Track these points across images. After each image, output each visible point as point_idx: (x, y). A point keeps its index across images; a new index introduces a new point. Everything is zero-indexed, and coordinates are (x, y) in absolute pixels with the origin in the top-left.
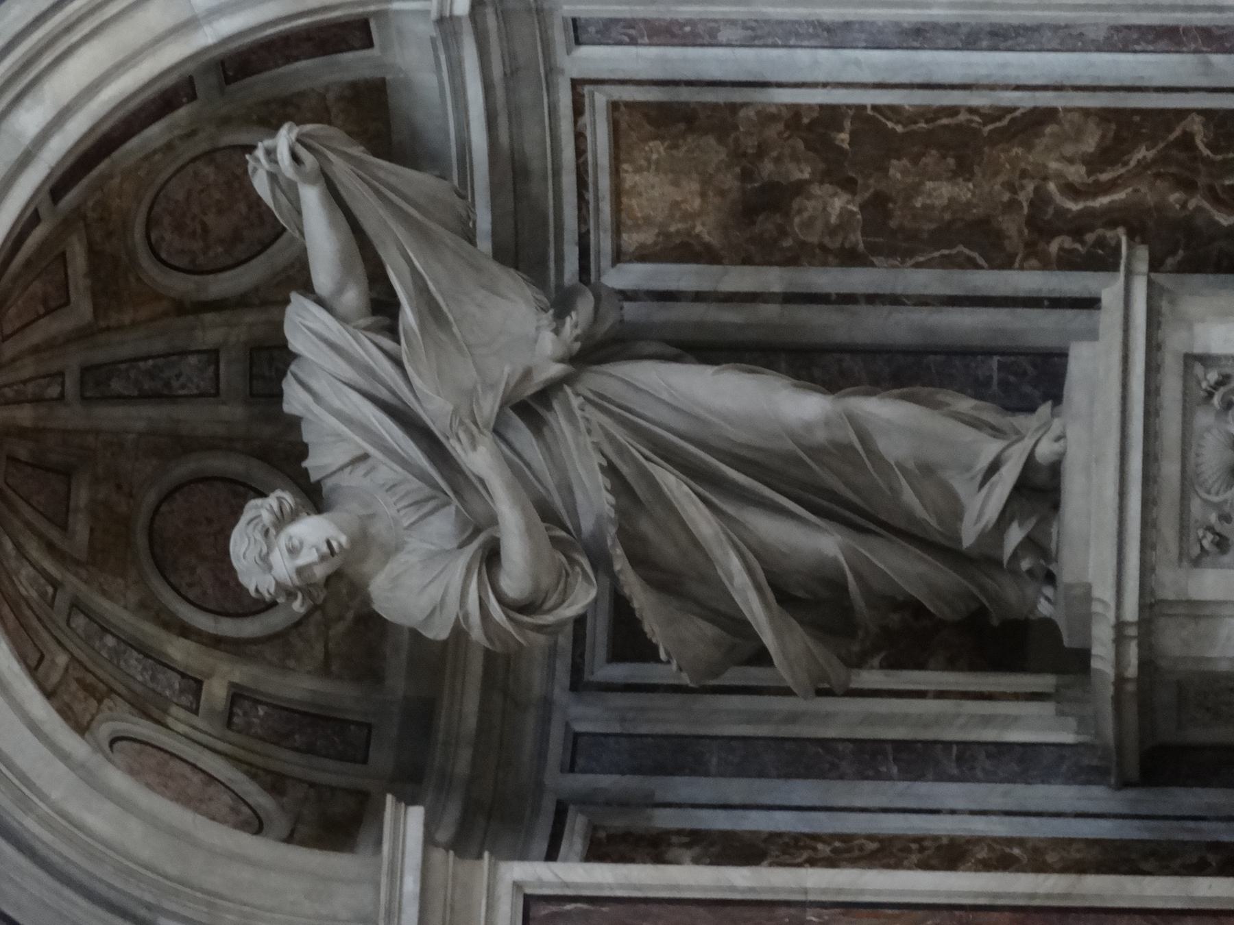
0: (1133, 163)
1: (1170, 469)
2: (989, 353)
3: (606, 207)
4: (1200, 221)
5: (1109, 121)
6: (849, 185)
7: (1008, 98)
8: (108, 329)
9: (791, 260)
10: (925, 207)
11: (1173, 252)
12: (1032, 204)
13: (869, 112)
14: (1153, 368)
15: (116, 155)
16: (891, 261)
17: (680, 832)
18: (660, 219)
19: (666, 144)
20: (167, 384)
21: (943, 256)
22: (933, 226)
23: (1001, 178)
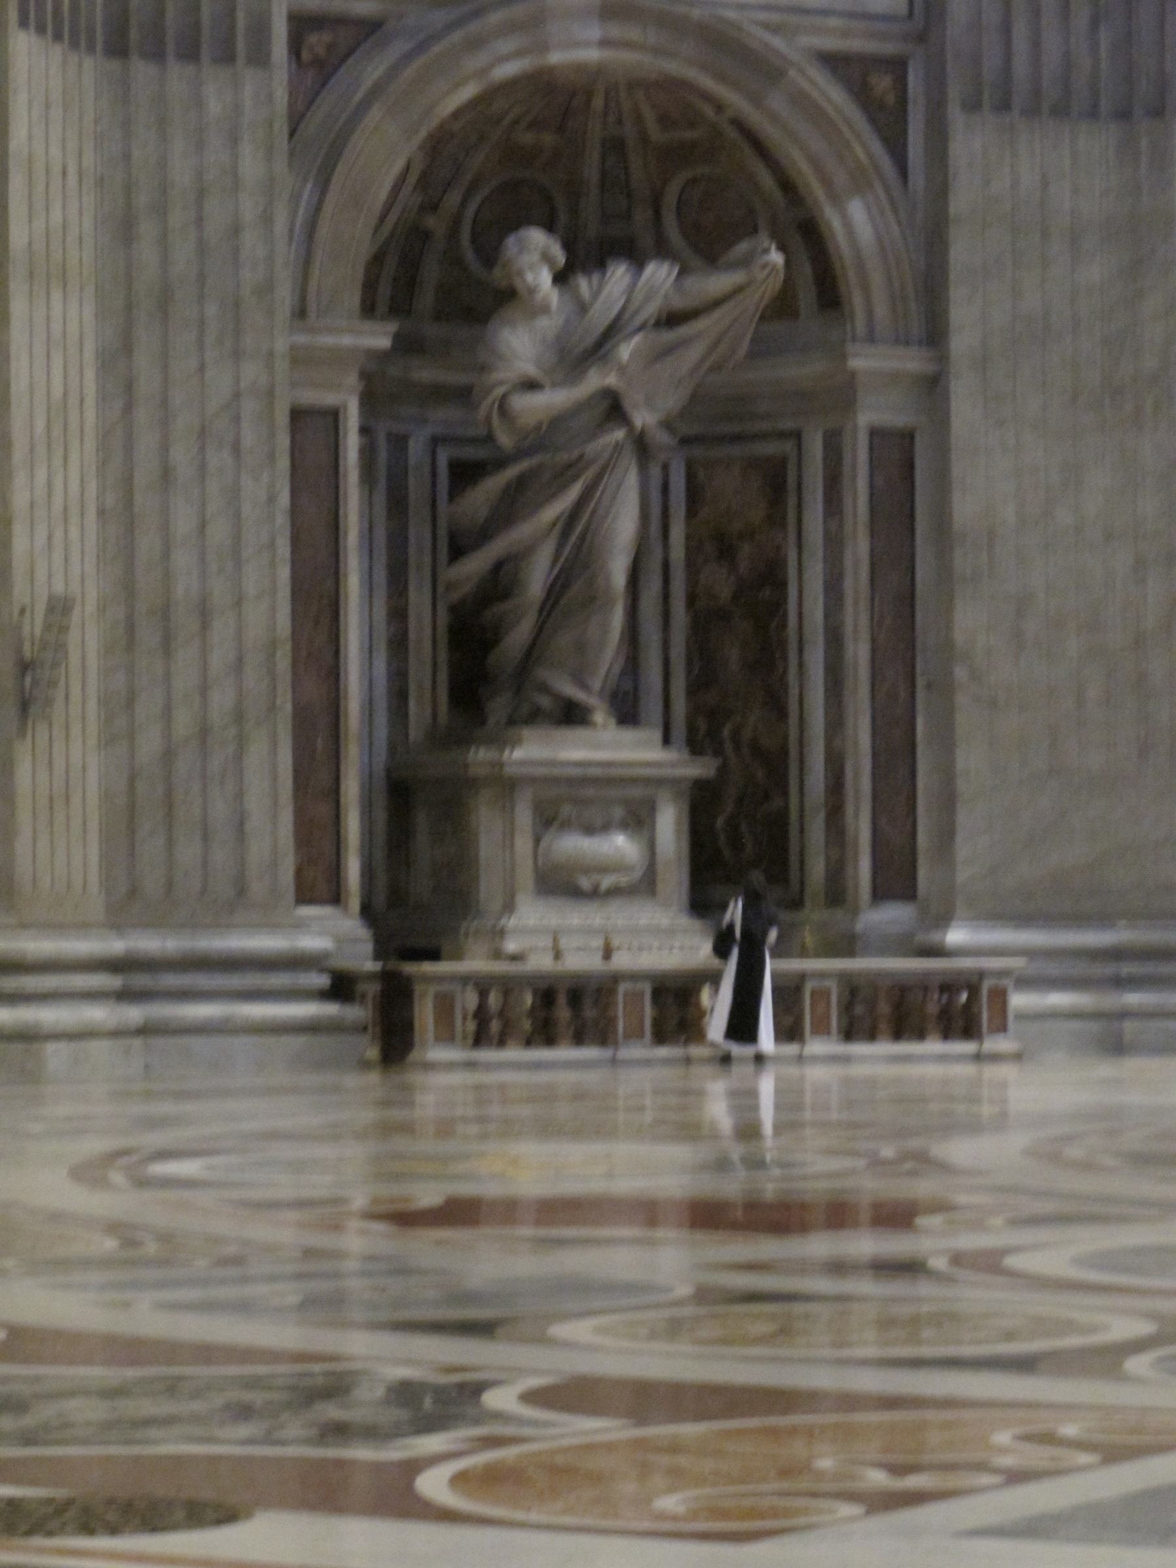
6: (735, 597)
7: (794, 692)
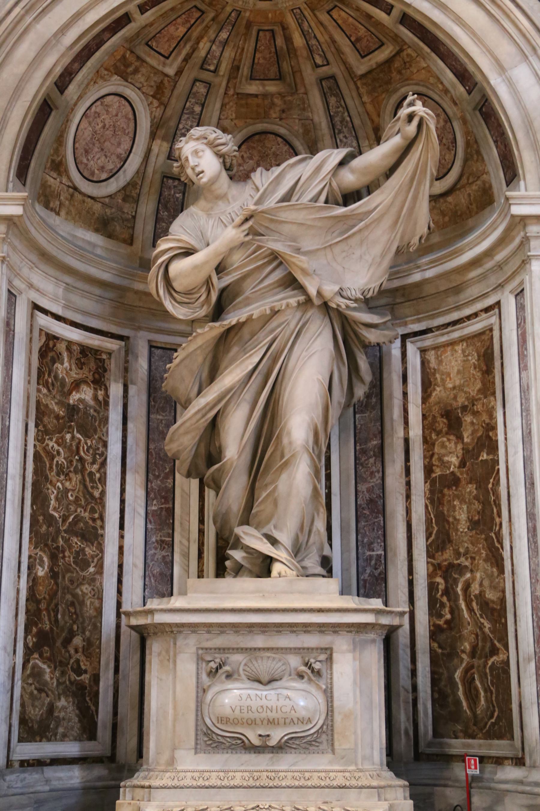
0: (482, 620)
1: (259, 641)
2: (385, 550)
3: (444, 339)
5: (501, 605)
6: (462, 464)
8: (358, 88)
9: (425, 441)
10: (454, 506)
11: (440, 647)
12: (459, 565)
13: (497, 468)
14: (322, 628)
15: (433, 55)
16: (428, 492)
17: (107, 395)
18: (441, 368)
19: (476, 363)
20: (340, 132)
21: (432, 519)
22: (445, 512)
23: (470, 546)
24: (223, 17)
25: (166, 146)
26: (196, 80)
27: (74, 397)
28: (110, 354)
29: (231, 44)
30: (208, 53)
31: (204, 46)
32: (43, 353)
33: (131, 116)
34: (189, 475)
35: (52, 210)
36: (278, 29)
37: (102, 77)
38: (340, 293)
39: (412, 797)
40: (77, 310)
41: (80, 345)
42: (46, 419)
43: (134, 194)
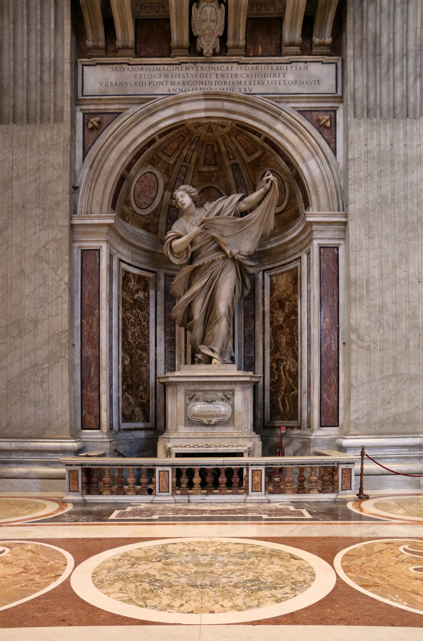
1: (207, 388)
4: (279, 394)
6: (284, 321)
9: (271, 312)
14: (230, 383)
17: (149, 295)
20: (240, 187)
24: (193, 139)
25: (170, 194)
26: (182, 166)
27: (136, 296)
28: (149, 278)
29: (196, 151)
30: (187, 154)
31: (185, 152)
32: (124, 279)
33: (156, 181)
34: (181, 326)
35: (126, 221)
36: (215, 144)
37: (144, 166)
38: (239, 253)
39: (261, 440)
40: (136, 261)
41: (138, 275)
42: (126, 305)
43: (158, 213)
